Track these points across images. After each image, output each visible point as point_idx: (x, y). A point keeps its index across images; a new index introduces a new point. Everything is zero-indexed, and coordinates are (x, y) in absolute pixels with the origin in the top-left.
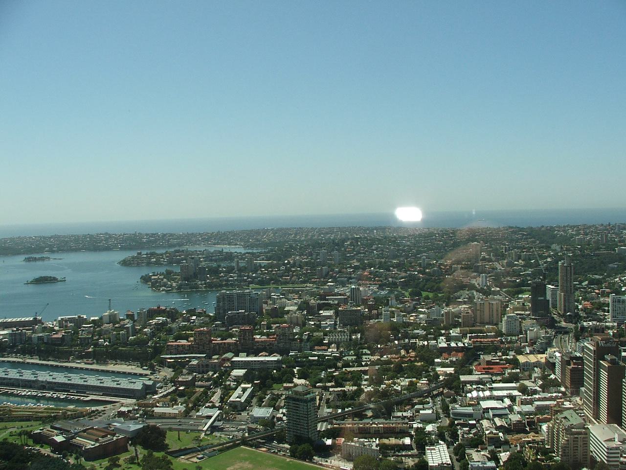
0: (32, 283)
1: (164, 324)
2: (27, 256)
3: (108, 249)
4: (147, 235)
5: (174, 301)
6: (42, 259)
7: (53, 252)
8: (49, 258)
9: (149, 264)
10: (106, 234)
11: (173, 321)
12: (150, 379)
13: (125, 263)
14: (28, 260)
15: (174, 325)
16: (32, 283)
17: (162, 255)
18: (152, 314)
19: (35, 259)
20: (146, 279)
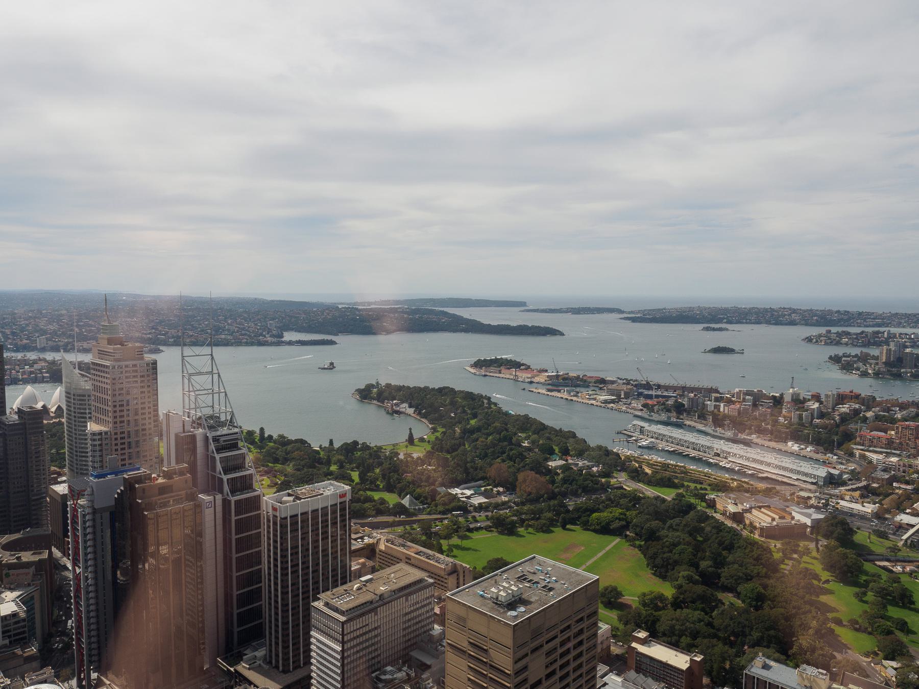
0: (710, 351)
1: (856, 412)
2: (706, 325)
3: (792, 323)
4: (838, 312)
5: (866, 387)
6: (720, 329)
7: (730, 322)
8: (727, 330)
9: (838, 343)
10: (790, 309)
11: (869, 409)
12: (835, 468)
13: (809, 340)
14: (707, 329)
15: (869, 414)
16: (710, 351)
17: (857, 334)
18: (841, 399)
19: (714, 329)
20: (835, 359)
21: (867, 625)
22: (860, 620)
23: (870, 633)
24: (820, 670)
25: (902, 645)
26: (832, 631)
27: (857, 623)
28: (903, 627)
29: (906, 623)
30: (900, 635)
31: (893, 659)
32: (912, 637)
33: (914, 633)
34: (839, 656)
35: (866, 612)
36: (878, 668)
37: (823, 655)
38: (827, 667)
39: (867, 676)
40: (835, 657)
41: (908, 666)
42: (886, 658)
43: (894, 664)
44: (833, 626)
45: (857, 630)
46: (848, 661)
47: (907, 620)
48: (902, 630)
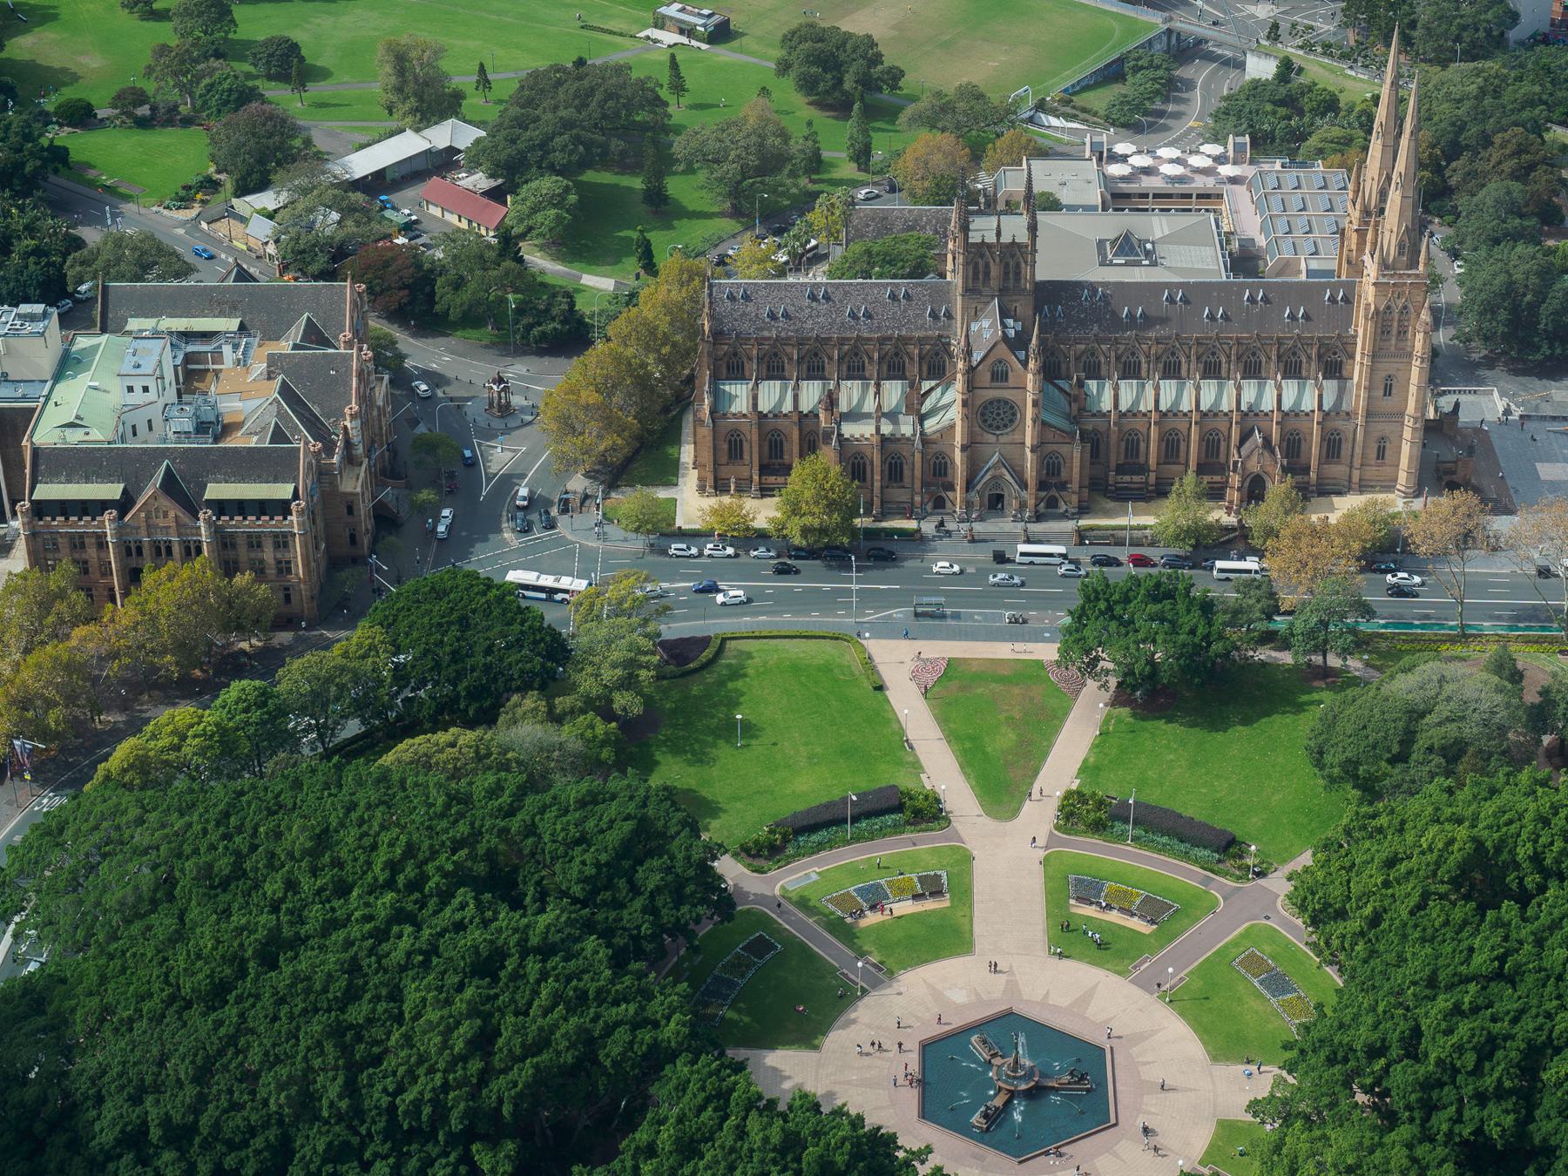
21: (174, 96)
22: (150, 87)
23: (187, 122)
24: (25, 308)
25: (283, 127)
26: (59, 155)
27: (140, 97)
28: (288, 63)
29: (294, 48)
30: (280, 96)
31: (262, 186)
32: (316, 90)
33: (322, 74)
34: (91, 235)
35: (163, 50)
36: (222, 228)
37: (37, 252)
38: (52, 290)
39: (185, 271)
40: (78, 243)
41: (305, 191)
42: (243, 190)
43: (267, 200)
44: (59, 135)
45: (143, 124)
46: (119, 242)
47: (297, 36)
48: (282, 77)
